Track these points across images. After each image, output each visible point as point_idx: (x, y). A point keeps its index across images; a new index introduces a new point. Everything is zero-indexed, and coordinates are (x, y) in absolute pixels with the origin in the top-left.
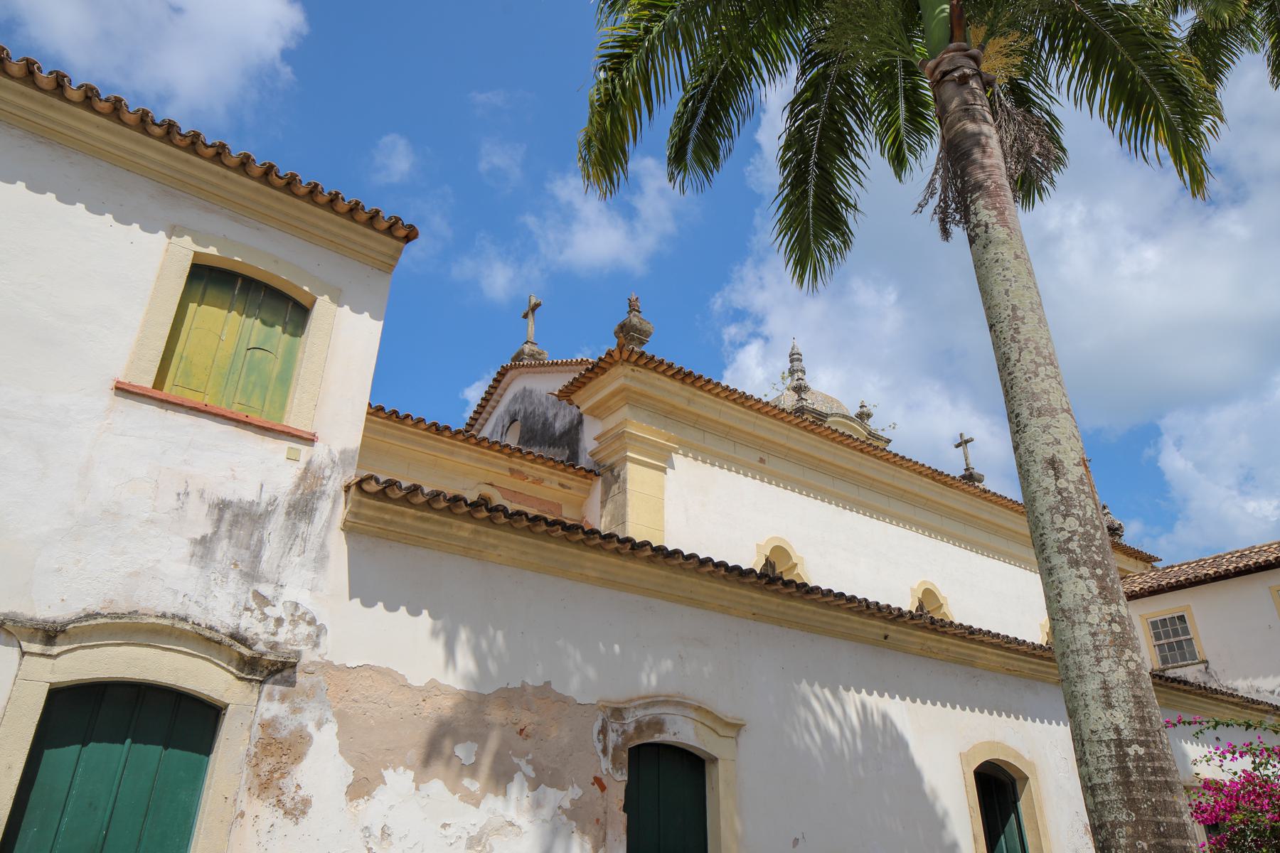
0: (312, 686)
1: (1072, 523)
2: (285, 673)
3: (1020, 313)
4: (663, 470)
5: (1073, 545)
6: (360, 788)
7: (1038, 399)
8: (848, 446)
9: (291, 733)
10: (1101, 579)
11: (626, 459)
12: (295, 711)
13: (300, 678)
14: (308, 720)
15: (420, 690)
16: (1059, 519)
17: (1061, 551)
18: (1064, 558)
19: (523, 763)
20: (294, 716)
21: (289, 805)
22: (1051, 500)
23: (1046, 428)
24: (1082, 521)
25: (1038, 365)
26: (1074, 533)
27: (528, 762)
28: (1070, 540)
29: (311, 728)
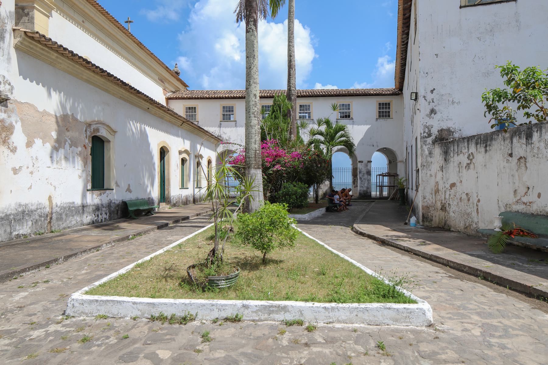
0: (13, 108)
1: (256, 109)
2: (4, 103)
4: (48, 17)
5: (255, 113)
6: (29, 144)
8: (115, 24)
9: (9, 124)
10: (258, 121)
11: (34, 7)
12: (9, 117)
13: (9, 105)
14: (13, 120)
15: (41, 113)
16: (254, 107)
17: (253, 114)
18: (253, 115)
19: (68, 139)
20: (8, 119)
21: (11, 148)
22: (253, 103)
23: (255, 87)
24: (258, 109)
27: (69, 139)
29: (14, 123)
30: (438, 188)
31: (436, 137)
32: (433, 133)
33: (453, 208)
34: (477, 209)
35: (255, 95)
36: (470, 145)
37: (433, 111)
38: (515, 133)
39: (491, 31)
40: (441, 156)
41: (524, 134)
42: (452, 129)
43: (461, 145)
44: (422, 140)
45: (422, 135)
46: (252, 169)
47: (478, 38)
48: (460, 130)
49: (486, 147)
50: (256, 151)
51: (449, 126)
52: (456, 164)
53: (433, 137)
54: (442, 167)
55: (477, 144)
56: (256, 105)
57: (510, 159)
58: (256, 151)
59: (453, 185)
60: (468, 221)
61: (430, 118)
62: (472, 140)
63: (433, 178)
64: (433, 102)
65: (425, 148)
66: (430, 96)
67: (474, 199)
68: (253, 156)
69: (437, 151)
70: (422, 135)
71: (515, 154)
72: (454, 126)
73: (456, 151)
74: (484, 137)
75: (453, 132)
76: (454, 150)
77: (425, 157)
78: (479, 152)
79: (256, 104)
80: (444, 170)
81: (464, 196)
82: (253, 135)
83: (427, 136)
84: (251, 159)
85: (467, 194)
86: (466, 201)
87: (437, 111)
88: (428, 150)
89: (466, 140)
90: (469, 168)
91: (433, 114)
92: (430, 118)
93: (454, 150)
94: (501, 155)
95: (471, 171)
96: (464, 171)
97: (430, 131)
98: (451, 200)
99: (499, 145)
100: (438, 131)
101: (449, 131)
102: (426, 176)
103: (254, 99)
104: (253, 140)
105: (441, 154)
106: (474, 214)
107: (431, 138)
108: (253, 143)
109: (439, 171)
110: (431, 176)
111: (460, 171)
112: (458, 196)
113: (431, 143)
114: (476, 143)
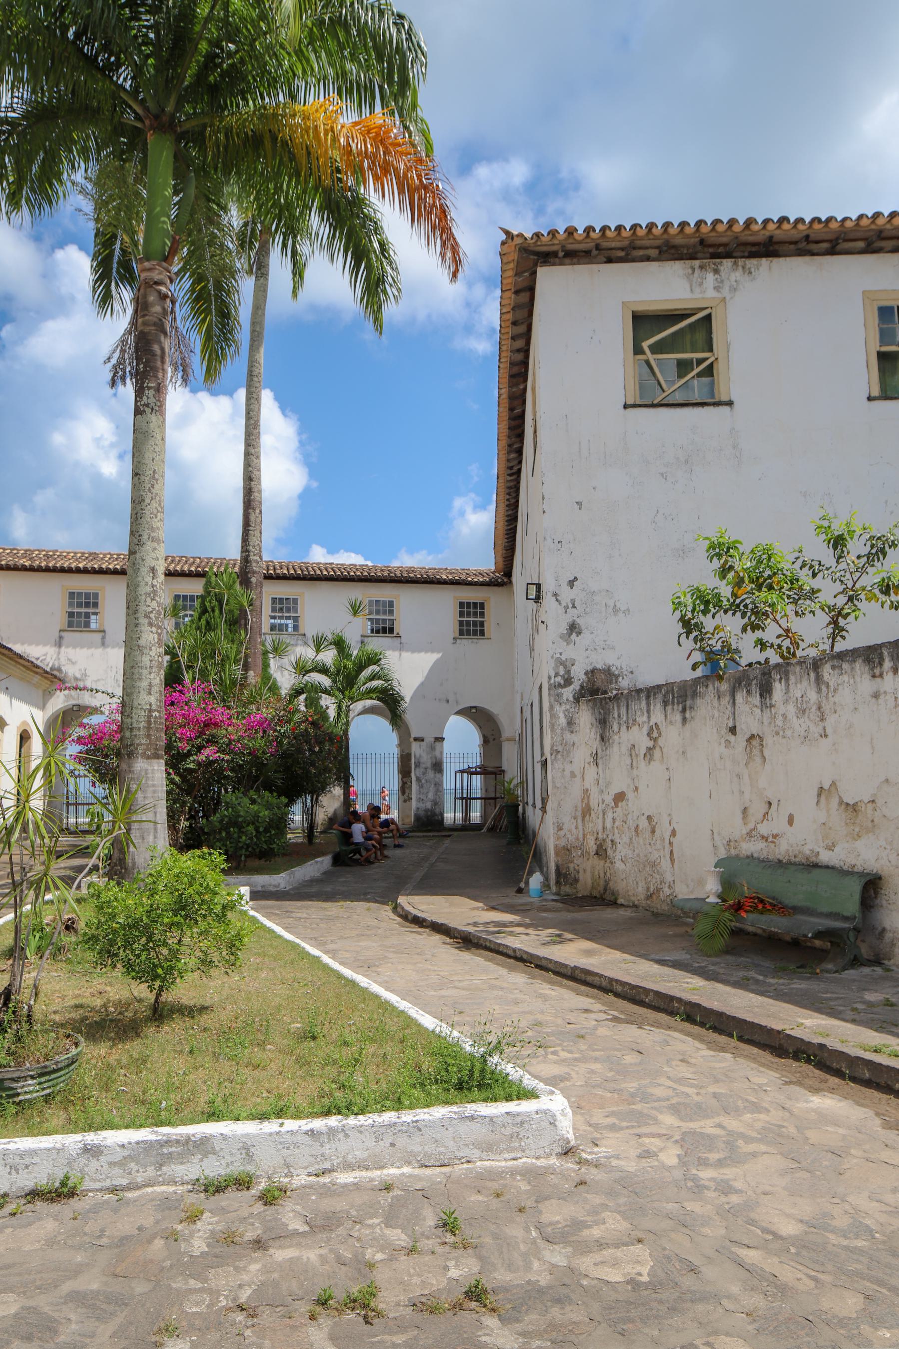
1: (154, 604)
3: (157, 476)
5: (152, 615)
7: (154, 531)
10: (159, 634)
16: (149, 600)
17: (146, 616)
18: (147, 620)
22: (148, 589)
23: (154, 549)
24: (159, 604)
25: (158, 511)
26: (154, 609)
28: (152, 612)
30: (588, 805)
31: (582, 687)
32: (576, 678)
33: (621, 852)
34: (672, 852)
35: (153, 570)
36: (652, 708)
37: (574, 628)
38: (740, 684)
39: (686, 462)
40: (594, 731)
41: (756, 685)
42: (614, 668)
43: (634, 706)
44: (552, 692)
45: (552, 682)
46: (140, 760)
47: (662, 474)
48: (632, 672)
49: (684, 711)
50: (150, 711)
51: (610, 662)
52: (625, 749)
53: (576, 686)
54: (597, 754)
55: (665, 704)
56: (155, 595)
57: (732, 738)
58: (150, 711)
59: (620, 797)
60: (654, 881)
61: (568, 644)
62: (655, 695)
63: (578, 779)
64: (574, 607)
65: (560, 711)
66: (567, 595)
67: (664, 830)
68: (142, 725)
69: (586, 717)
70: (552, 682)
71: (742, 729)
72: (618, 663)
73: (625, 719)
74: (680, 689)
75: (617, 677)
76: (619, 716)
77: (558, 731)
78: (671, 722)
79: (155, 592)
80: (600, 762)
81: (644, 824)
82: (145, 672)
83: (562, 682)
84: (135, 732)
85: (649, 818)
86: (648, 834)
87: (583, 627)
88: (566, 716)
89: (643, 695)
90: (651, 760)
91: (574, 634)
92: (568, 644)
93: (619, 716)
94: (715, 731)
95: (656, 765)
96: (642, 764)
97: (569, 671)
98: (616, 831)
99: (709, 708)
100: (586, 673)
101: (608, 671)
102: (563, 777)
103: (149, 579)
104: (144, 684)
105: (592, 725)
106: (665, 864)
107: (572, 687)
108: (142, 692)
109: (589, 763)
110: (573, 775)
111: (634, 764)
112: (631, 824)
113: (572, 700)
114: (664, 702)
